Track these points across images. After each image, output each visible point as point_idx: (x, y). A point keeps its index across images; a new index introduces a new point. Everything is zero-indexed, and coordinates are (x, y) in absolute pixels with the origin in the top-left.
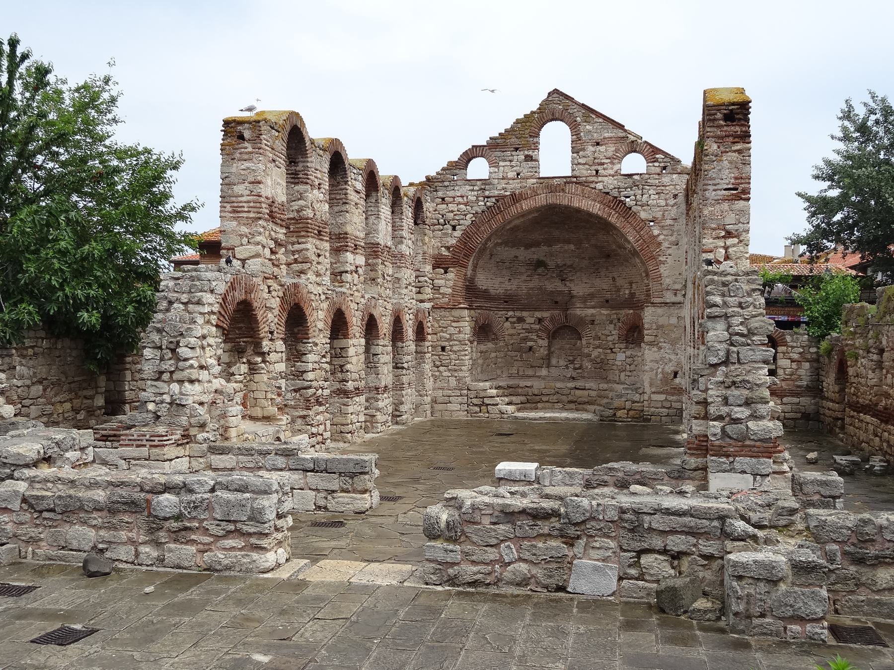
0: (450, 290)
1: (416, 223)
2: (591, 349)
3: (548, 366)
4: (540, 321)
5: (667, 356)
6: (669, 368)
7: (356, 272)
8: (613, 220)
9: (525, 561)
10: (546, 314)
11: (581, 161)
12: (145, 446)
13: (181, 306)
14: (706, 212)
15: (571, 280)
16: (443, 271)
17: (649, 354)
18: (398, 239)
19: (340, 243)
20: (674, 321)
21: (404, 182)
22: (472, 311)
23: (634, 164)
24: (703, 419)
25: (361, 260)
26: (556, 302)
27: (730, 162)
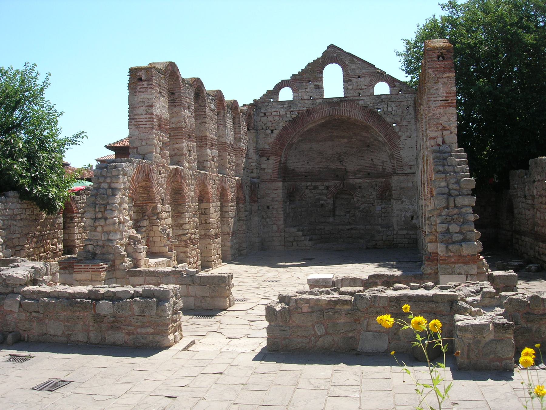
0: (270, 171)
1: (248, 130)
2: (360, 204)
3: (334, 215)
4: (327, 188)
5: (407, 206)
6: (408, 214)
7: (213, 160)
8: (370, 124)
9: (331, 334)
10: (331, 183)
11: (349, 87)
12: (89, 271)
13: (106, 184)
15: (346, 162)
16: (265, 159)
17: (396, 206)
18: (238, 140)
19: (202, 142)
20: (410, 185)
21: (240, 104)
22: (286, 183)
23: (382, 89)
24: (434, 242)
25: (216, 152)
26: (337, 176)
27: (442, 83)
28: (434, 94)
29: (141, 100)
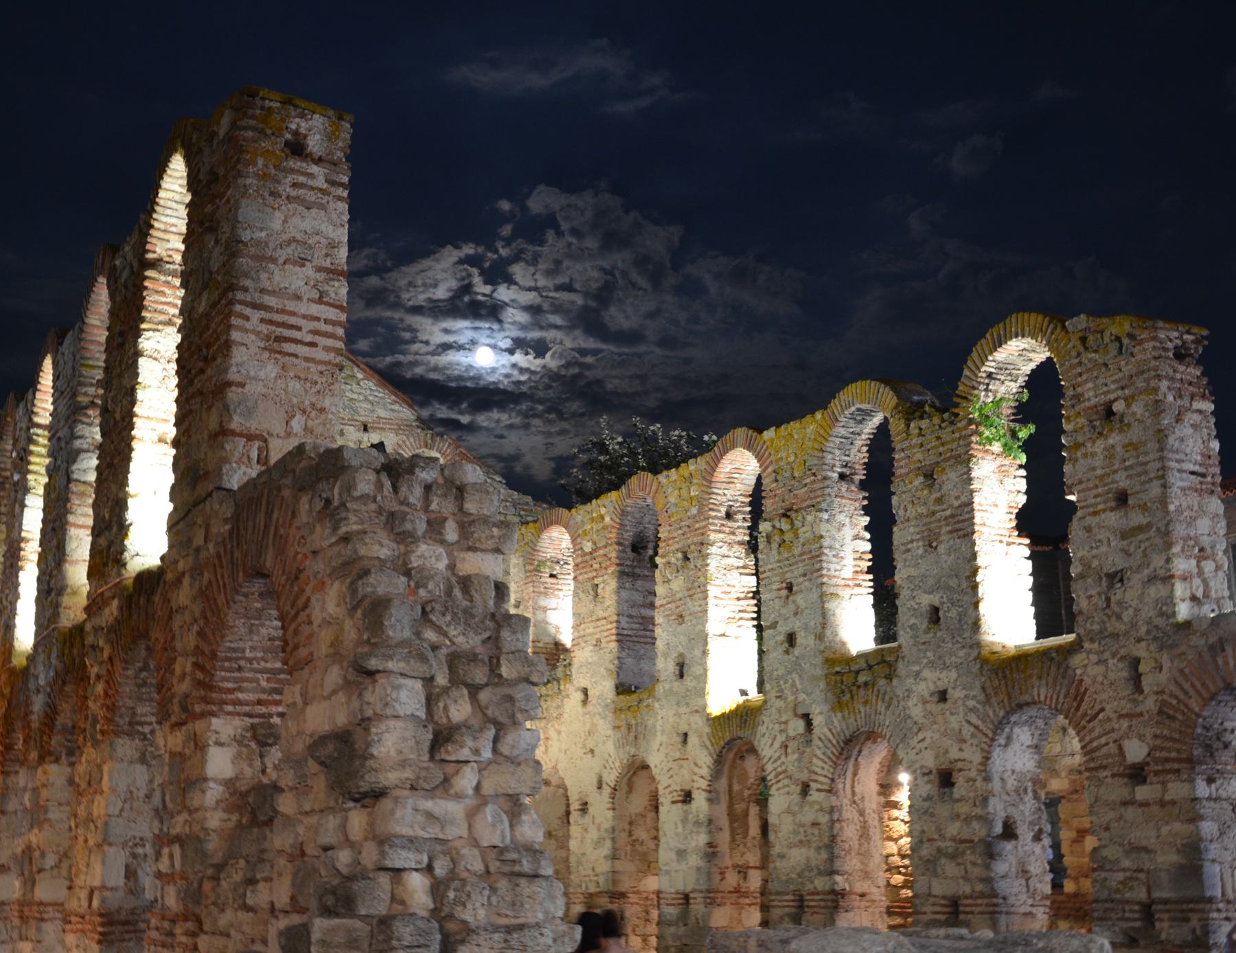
13: (441, 550)
14: (1172, 508)
28: (1177, 452)
29: (299, 236)
